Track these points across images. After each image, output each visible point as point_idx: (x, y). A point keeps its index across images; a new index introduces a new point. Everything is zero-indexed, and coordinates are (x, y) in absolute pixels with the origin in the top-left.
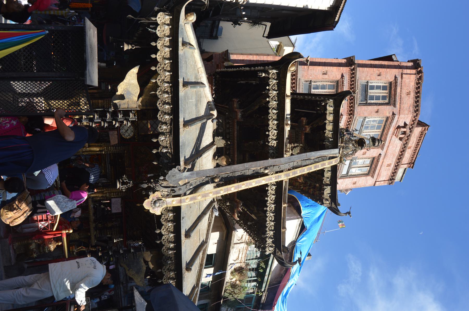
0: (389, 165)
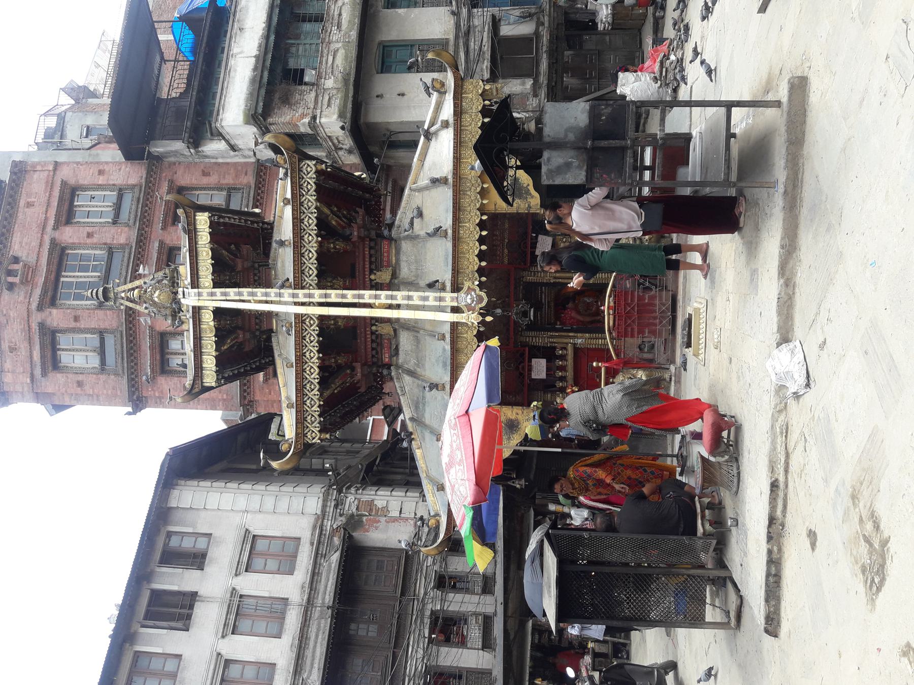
0: (29, 205)
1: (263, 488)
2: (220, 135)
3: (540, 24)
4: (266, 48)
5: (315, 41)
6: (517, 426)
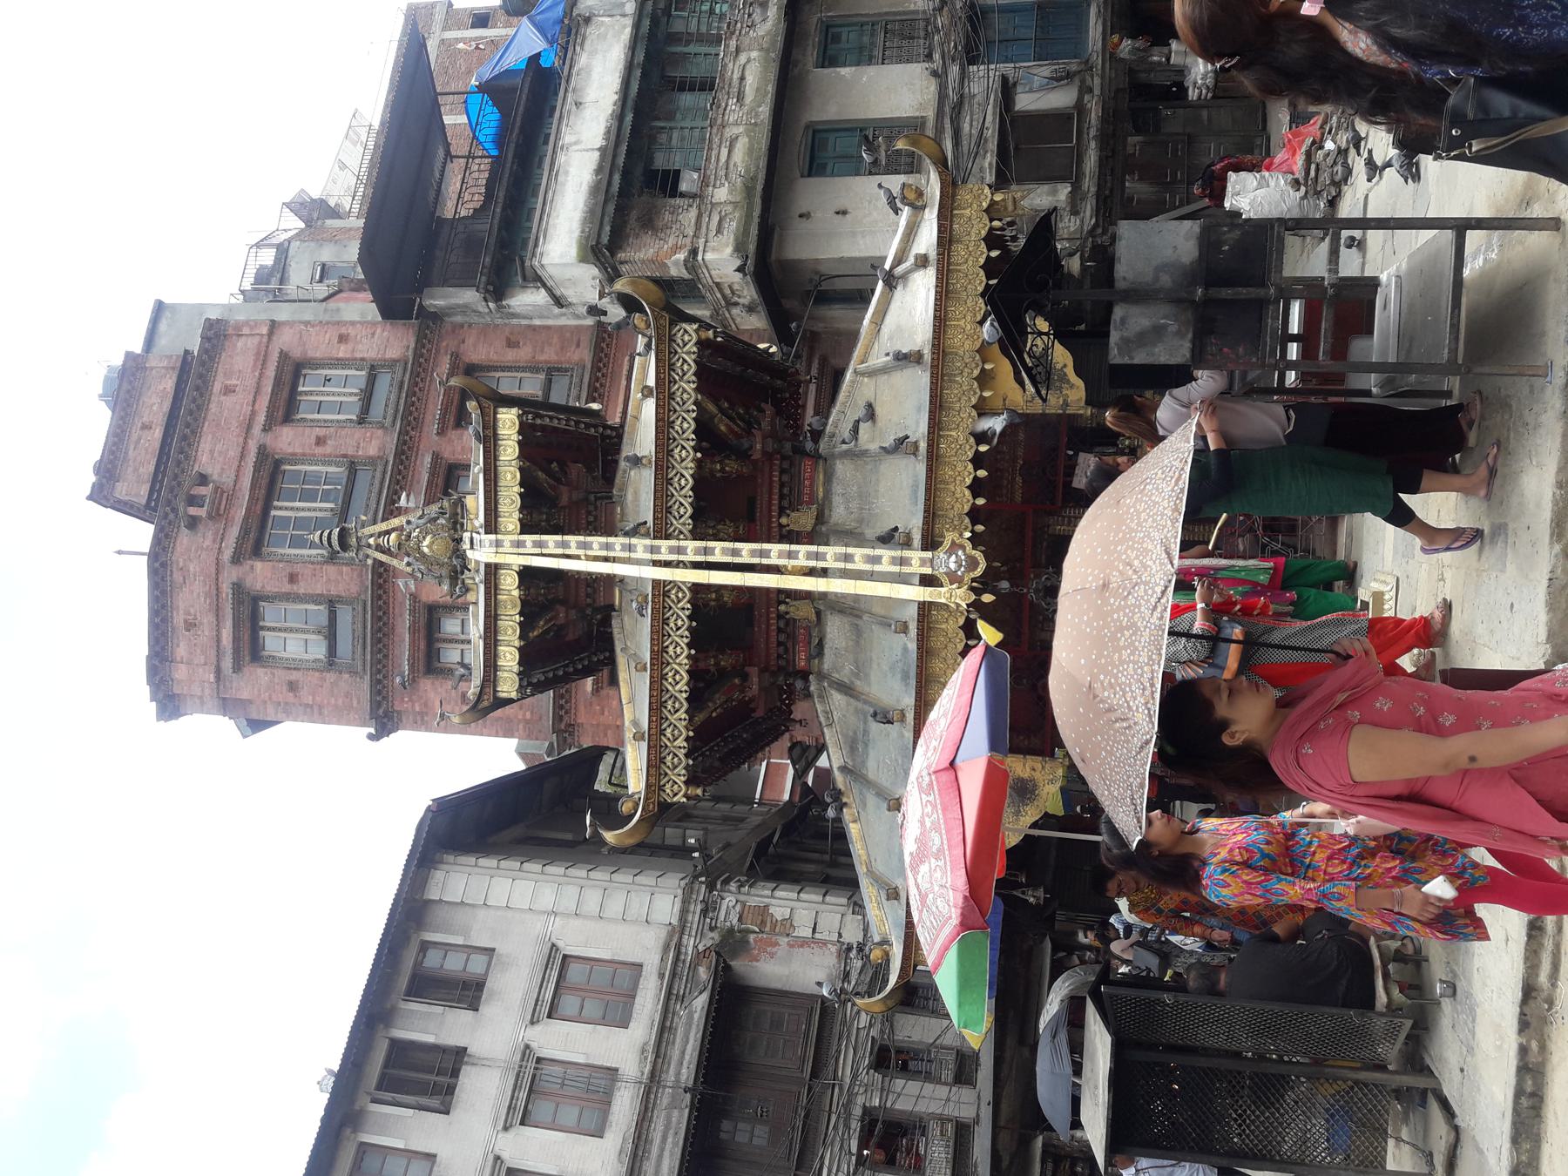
0: (228, 390)
1: (583, 873)
2: (538, 280)
3: (1085, 90)
4: (618, 136)
5: (701, 124)
6: (1033, 792)
